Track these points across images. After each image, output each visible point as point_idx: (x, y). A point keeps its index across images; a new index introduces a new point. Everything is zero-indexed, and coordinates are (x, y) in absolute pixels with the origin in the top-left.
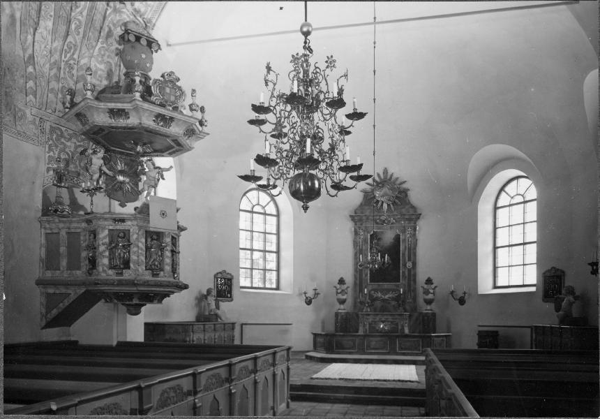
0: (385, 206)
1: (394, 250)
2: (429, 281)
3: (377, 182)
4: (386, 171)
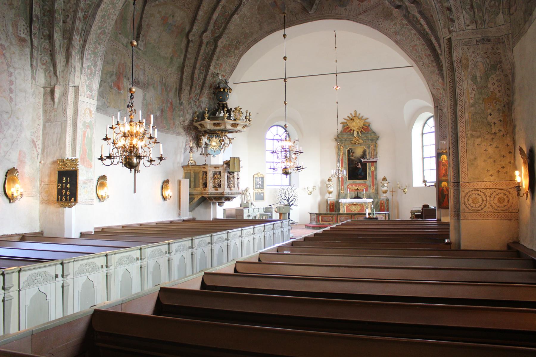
0: (355, 133)
2: (385, 179)
4: (356, 112)
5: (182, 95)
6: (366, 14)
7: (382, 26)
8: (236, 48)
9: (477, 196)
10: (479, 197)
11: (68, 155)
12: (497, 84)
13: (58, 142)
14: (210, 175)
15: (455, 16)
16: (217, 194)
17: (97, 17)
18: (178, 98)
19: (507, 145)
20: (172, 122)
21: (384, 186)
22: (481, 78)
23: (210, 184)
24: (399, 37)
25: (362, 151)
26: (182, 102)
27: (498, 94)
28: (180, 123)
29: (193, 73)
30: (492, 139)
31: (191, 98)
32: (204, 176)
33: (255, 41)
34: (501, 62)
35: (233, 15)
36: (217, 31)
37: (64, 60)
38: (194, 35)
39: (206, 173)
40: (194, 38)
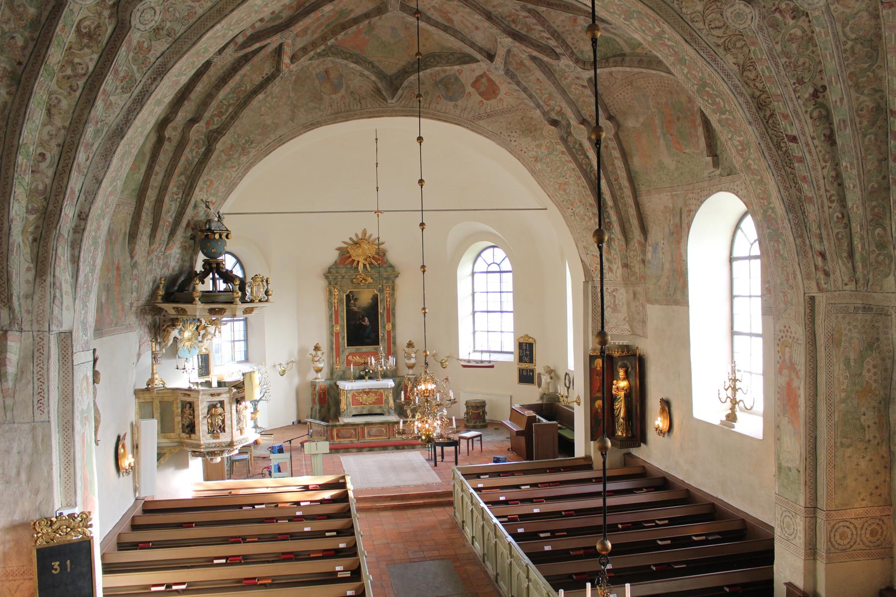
0: (361, 266)
1: (373, 310)
2: (410, 345)
3: (353, 241)
5: (137, 247)
6: (490, 120)
7: (515, 144)
8: (244, 151)
9: (845, 529)
10: (848, 530)
11: (58, 505)
12: (873, 370)
13: (23, 476)
14: (202, 409)
15: (831, 267)
16: (220, 445)
17: (115, 161)
18: (128, 254)
19: (883, 457)
20: (120, 307)
21: (409, 357)
22: (855, 362)
23: (202, 427)
24: (539, 166)
25: (371, 296)
26: (136, 262)
27: (874, 385)
28: (131, 304)
29: (159, 202)
30: (866, 448)
31: (153, 251)
32: (187, 411)
33: (281, 141)
34: (878, 339)
35: (255, 92)
36: (215, 119)
37: (27, 265)
38: (175, 129)
39: (191, 405)
40: (174, 133)
